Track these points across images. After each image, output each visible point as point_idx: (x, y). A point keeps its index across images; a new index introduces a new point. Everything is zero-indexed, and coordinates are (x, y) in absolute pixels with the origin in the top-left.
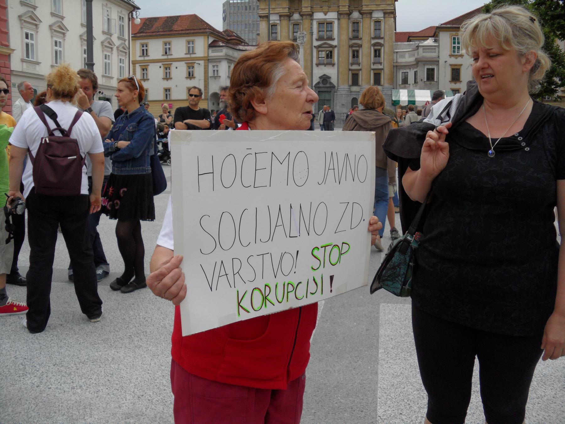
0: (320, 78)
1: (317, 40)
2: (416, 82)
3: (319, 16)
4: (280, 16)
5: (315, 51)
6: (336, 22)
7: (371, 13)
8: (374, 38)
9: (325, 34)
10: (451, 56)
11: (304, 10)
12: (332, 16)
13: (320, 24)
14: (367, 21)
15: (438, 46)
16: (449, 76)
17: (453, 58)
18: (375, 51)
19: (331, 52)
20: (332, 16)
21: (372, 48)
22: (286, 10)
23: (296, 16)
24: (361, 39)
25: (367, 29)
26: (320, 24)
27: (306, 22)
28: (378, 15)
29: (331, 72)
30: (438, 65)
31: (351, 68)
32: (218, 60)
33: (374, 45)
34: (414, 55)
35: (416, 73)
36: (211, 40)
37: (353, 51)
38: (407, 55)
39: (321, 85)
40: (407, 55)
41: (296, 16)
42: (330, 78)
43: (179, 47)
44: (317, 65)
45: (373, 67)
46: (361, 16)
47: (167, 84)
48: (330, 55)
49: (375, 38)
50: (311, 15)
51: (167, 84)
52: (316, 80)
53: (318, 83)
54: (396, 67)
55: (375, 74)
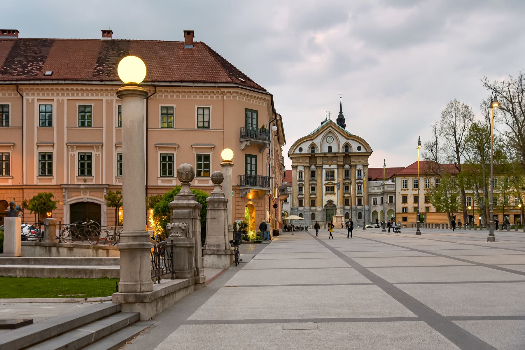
0: (327, 202)
2: (382, 203)
3: (326, 167)
4: (304, 167)
6: (336, 170)
7: (356, 166)
10: (402, 190)
11: (318, 163)
12: (334, 167)
13: (327, 171)
14: (353, 170)
15: (395, 185)
16: (401, 201)
17: (403, 191)
18: (358, 186)
19: (333, 187)
20: (334, 167)
22: (308, 164)
23: (313, 167)
25: (353, 174)
26: (327, 171)
27: (319, 171)
28: (360, 167)
29: (333, 198)
30: (395, 194)
33: (358, 183)
34: (380, 189)
35: (382, 198)
38: (376, 188)
39: (328, 206)
40: (376, 188)
41: (313, 167)
44: (326, 194)
45: (357, 195)
48: (333, 188)
49: (358, 179)
50: (322, 167)
52: (325, 203)
53: (327, 205)
55: (358, 199)
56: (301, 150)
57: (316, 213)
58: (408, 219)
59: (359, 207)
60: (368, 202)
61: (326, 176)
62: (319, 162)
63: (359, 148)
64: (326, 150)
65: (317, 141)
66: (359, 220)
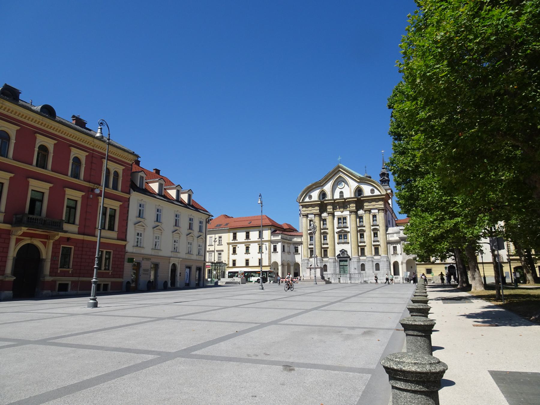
0: (340, 251)
1: (337, 228)
3: (338, 213)
5: (336, 236)
8: (372, 226)
9: (342, 225)
12: (346, 213)
14: (367, 215)
21: (372, 232)
24: (364, 227)
25: (367, 219)
26: (339, 219)
31: (360, 244)
32: (277, 242)
33: (374, 230)
36: (273, 229)
37: (361, 235)
39: (341, 256)
42: (346, 251)
43: (254, 235)
44: (338, 243)
45: (373, 243)
46: (364, 212)
47: (247, 257)
48: (345, 237)
51: (247, 257)
52: (338, 253)
53: (339, 255)
54: (389, 243)
56: (310, 197)
57: (328, 264)
58: (433, 271)
59: (376, 257)
60: (387, 252)
61: (339, 223)
62: (330, 208)
63: (372, 191)
64: (337, 196)
65: (327, 188)
66: (377, 272)
